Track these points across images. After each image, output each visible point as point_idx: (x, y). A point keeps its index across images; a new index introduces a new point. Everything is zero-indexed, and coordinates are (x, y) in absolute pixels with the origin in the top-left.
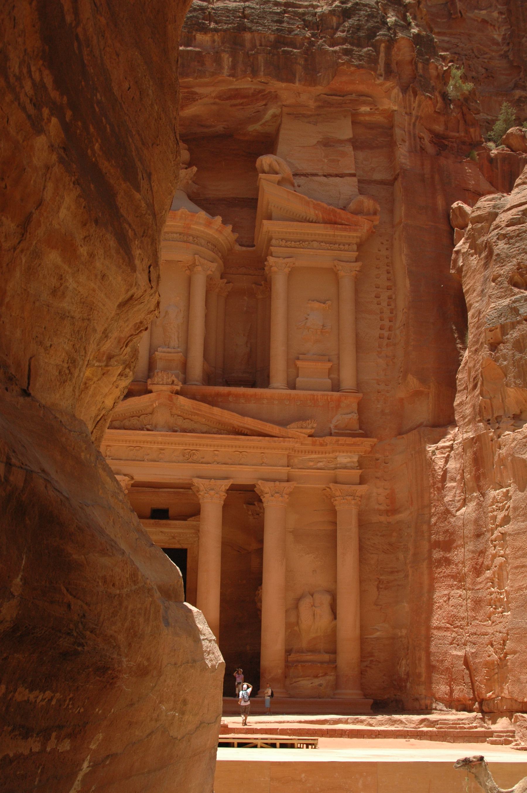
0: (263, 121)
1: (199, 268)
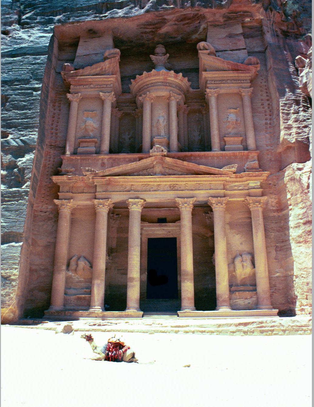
0: (199, 33)
1: (173, 98)
